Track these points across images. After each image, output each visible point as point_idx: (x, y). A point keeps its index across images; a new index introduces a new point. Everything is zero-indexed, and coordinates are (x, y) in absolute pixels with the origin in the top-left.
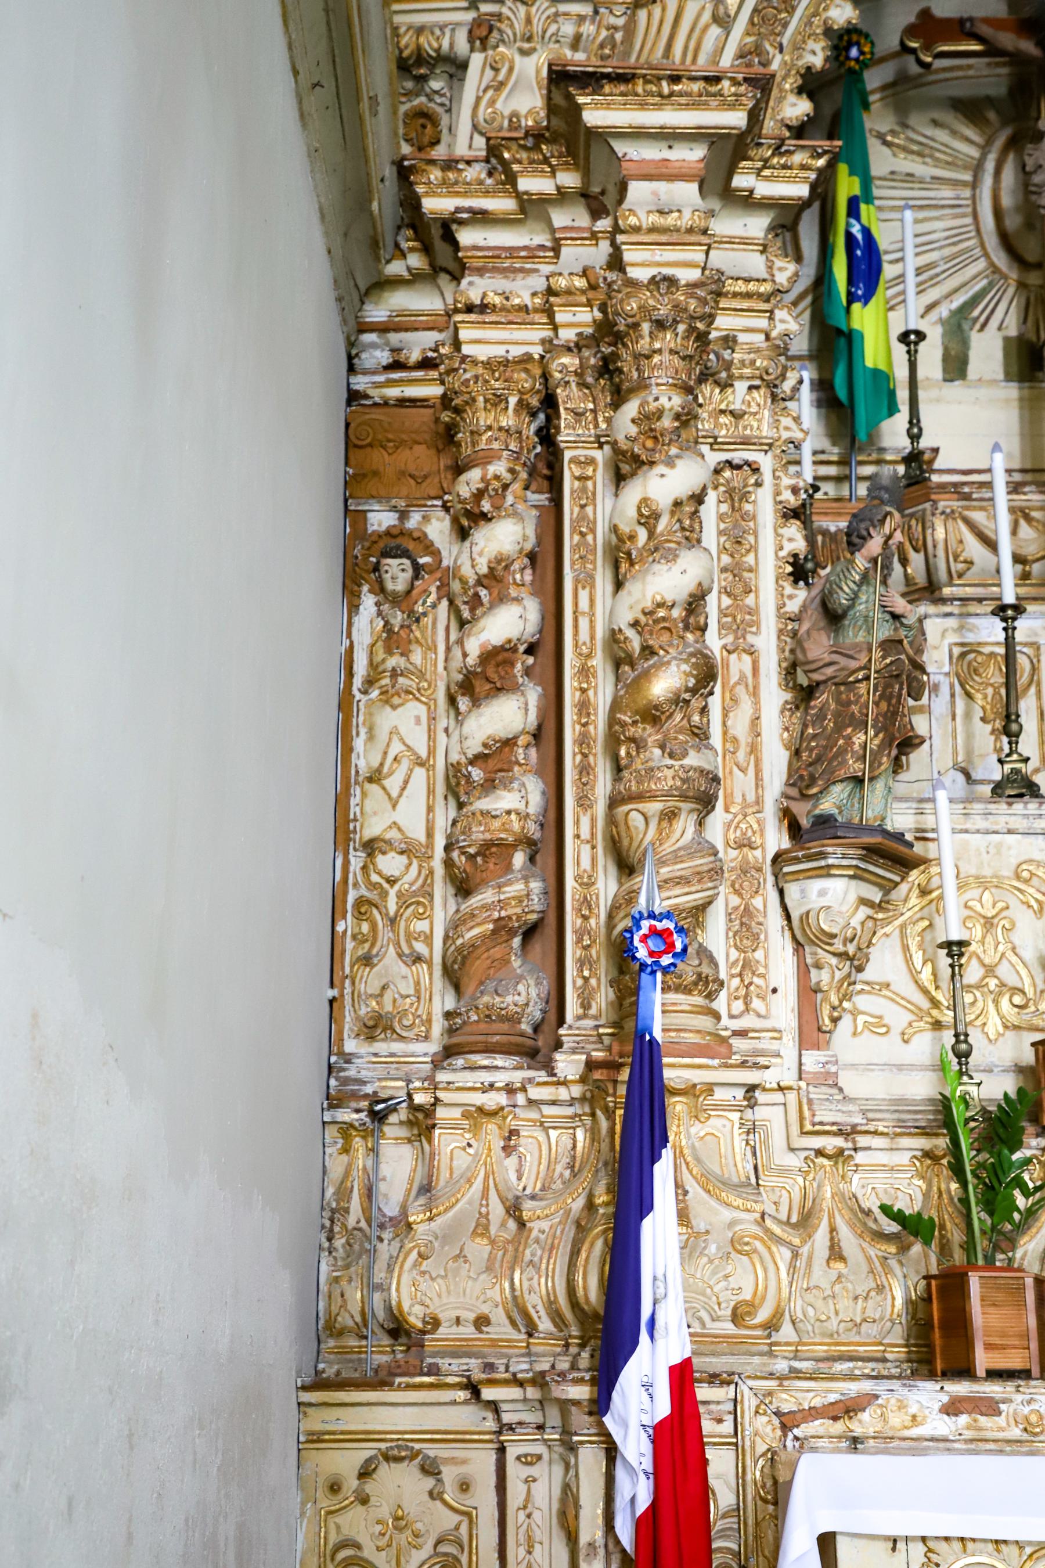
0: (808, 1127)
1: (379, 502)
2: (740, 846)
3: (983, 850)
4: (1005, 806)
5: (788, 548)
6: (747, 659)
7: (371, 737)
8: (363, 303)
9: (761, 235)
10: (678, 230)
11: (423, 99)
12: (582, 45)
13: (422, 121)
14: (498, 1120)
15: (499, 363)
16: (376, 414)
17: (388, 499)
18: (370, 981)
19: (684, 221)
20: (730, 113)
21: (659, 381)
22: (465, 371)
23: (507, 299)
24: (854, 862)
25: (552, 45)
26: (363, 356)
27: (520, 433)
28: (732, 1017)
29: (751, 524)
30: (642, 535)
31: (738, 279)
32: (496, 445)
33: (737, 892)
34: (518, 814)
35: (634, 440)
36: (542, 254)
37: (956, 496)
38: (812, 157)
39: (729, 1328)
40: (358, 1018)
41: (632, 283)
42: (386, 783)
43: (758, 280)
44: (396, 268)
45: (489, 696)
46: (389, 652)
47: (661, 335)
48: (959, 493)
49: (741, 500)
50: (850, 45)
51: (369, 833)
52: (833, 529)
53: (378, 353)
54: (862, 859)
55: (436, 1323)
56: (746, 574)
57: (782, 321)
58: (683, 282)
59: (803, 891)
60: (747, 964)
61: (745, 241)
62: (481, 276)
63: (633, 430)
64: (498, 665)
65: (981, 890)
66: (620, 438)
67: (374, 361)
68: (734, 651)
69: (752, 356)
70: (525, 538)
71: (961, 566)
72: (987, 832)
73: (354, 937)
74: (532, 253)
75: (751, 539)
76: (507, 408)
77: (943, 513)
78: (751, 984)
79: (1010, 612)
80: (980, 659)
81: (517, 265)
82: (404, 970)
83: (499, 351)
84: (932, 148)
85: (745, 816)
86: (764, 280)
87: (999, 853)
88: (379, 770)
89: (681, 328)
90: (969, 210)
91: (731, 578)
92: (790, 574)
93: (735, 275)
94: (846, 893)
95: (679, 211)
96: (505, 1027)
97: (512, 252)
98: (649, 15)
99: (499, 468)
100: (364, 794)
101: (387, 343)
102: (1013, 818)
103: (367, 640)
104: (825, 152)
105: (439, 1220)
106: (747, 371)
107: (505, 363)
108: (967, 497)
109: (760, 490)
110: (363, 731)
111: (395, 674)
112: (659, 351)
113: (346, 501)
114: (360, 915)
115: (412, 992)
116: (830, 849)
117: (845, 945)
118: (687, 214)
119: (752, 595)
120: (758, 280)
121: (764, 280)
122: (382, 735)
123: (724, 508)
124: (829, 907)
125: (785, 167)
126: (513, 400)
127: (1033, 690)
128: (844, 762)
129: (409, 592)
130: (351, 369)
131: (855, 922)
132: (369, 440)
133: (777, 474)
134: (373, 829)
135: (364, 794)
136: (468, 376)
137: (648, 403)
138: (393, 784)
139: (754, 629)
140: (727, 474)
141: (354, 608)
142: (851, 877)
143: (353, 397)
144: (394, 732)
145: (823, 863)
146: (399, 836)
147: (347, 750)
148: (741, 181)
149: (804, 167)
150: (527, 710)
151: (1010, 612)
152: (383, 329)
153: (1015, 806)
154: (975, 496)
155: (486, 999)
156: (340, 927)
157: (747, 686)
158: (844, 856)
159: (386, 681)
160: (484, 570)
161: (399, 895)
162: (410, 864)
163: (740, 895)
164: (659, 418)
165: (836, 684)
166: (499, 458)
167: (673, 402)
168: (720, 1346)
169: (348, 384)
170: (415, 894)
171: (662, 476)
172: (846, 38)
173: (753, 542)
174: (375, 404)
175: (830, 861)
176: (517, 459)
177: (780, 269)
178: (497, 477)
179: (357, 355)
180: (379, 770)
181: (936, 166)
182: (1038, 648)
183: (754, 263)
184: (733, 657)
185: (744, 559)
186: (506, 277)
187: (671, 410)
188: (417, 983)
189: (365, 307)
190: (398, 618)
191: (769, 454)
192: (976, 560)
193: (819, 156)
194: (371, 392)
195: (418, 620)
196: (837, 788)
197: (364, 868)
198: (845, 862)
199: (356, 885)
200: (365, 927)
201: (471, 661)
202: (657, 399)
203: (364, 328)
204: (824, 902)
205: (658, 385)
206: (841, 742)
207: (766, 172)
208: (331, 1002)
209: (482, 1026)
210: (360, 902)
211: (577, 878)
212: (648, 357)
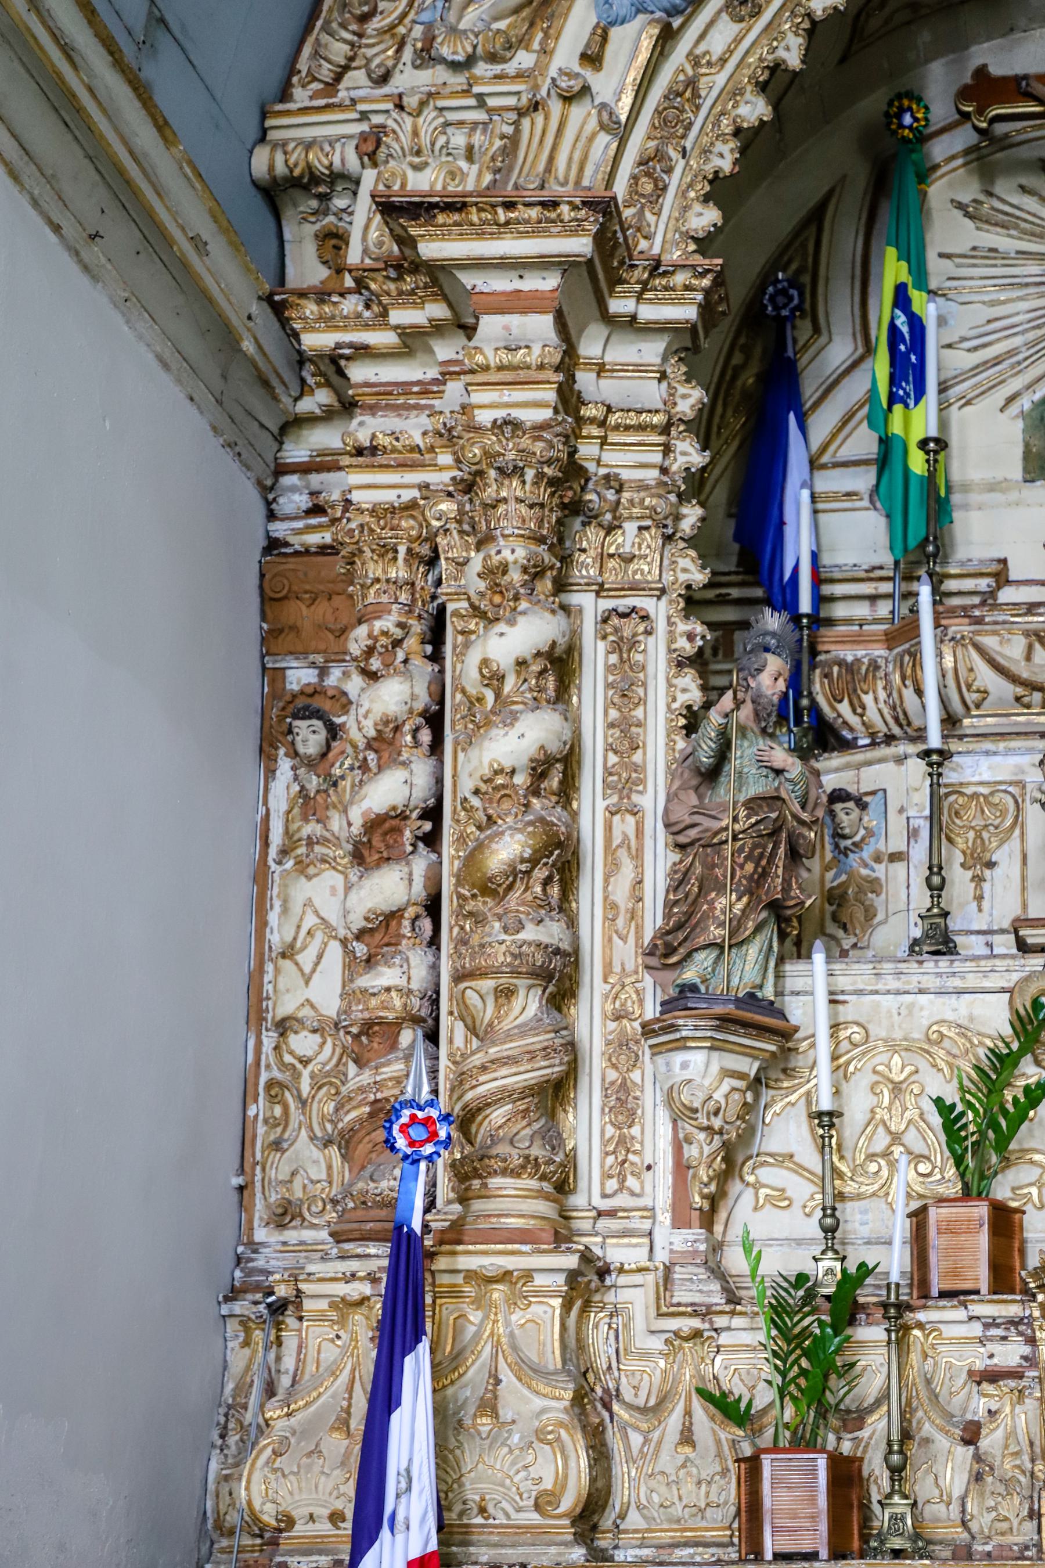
0: (664, 1309)
1: (297, 659)
2: (618, 1018)
3: (895, 1012)
4: (916, 965)
5: (682, 699)
6: (631, 820)
7: (285, 910)
8: (281, 443)
9: (658, 361)
10: (529, 367)
11: (331, 218)
12: (476, 157)
13: (334, 242)
14: (364, 1310)
15: (386, 510)
16: (292, 563)
17: (306, 653)
18: (280, 1167)
19: (534, 357)
20: (574, 239)
21: (506, 532)
22: (349, 520)
23: (397, 439)
24: (709, 1034)
25: (444, 159)
26: (281, 500)
27: (413, 584)
28: (604, 1196)
29: (641, 675)
30: (490, 696)
31: (629, 411)
32: (385, 599)
33: (614, 1066)
34: (399, 991)
35: (482, 595)
36: (435, 389)
38: (695, 277)
39: (535, 1518)
40: (268, 1206)
41: (477, 429)
42: (299, 958)
43: (650, 411)
44: (307, 405)
45: (378, 865)
46: (306, 819)
47: (506, 482)
49: (629, 651)
51: (282, 1012)
52: (850, 658)
53: (296, 497)
54: (717, 1029)
55: (290, 1522)
56: (634, 729)
57: (684, 454)
58: (528, 424)
59: (668, 1064)
60: (622, 1141)
61: (638, 368)
62: (373, 415)
63: (482, 585)
64: (386, 834)
65: (890, 1054)
66: (472, 593)
67: (293, 505)
68: (616, 813)
69: (642, 494)
70: (413, 697)
71: (975, 696)
72: (898, 993)
73: (266, 1121)
74: (426, 389)
75: (641, 691)
76: (395, 559)
77: (953, 639)
78: (624, 1161)
79: (935, 758)
80: (961, 801)
81: (411, 402)
82: (316, 1153)
83: (388, 496)
85: (623, 986)
86: (657, 411)
87: (910, 1014)
88: (292, 946)
89: (530, 474)
91: (618, 733)
92: (684, 727)
93: (625, 406)
94: (707, 1065)
95: (527, 347)
96: (383, 1213)
97: (405, 388)
98: (533, 123)
99: (387, 623)
100: (277, 971)
101: (307, 487)
102: (926, 977)
103: (284, 807)
104: (708, 271)
105: (299, 1416)
106: (636, 511)
107: (392, 510)
109: (651, 639)
110: (277, 904)
111: (310, 842)
112: (505, 500)
113: (263, 657)
114: (272, 1099)
115: (323, 1176)
116: (681, 1022)
117: (708, 1119)
118: (536, 350)
119: (640, 751)
120: (650, 411)
121: (657, 411)
122: (296, 908)
123: (614, 659)
124: (690, 1081)
125: (666, 288)
126: (402, 550)
127: (1017, 832)
128: (707, 928)
129: (324, 755)
130: (271, 516)
131: (719, 1096)
132: (285, 592)
133: (673, 620)
134: (286, 1006)
135: (277, 971)
136: (353, 525)
137: (490, 556)
138: (306, 958)
139: (641, 788)
140: (615, 621)
141: (271, 773)
142: (711, 1048)
143: (273, 545)
144: (308, 903)
145: (678, 1035)
146: (312, 1013)
147: (262, 924)
148: (620, 305)
149: (687, 288)
150: (411, 881)
151: (935, 758)
152: (305, 469)
153: (925, 965)
155: (360, 1185)
156: (251, 1112)
157: (629, 848)
158: (696, 1028)
159: (302, 850)
160: (372, 733)
161: (312, 1076)
162: (324, 1043)
163: (617, 1068)
164: (505, 572)
165: (703, 846)
166: (389, 612)
167: (516, 554)
168: (523, 1537)
169: (267, 532)
170: (328, 1074)
171: (502, 634)
173: (642, 695)
174: (297, 553)
175: (684, 1033)
176: (410, 611)
177: (684, 397)
178: (385, 633)
179: (274, 500)
180: (292, 946)
182: (1024, 787)
183: (652, 393)
184: (617, 818)
185: (633, 713)
186: (399, 415)
187: (515, 562)
188: (330, 1167)
189: (285, 447)
190: (314, 783)
191: (664, 599)
192: (990, 689)
193: (702, 275)
194: (291, 539)
195: (335, 784)
196: (700, 956)
197: (277, 1048)
198: (699, 1034)
199: (268, 1066)
200: (278, 1111)
201: (356, 829)
202: (499, 552)
203: (281, 470)
204: (687, 1075)
205: (503, 536)
206: (705, 907)
207: (648, 295)
208: (241, 1189)
209: (360, 1214)
210: (271, 1084)
211: (451, 1055)
212: (494, 507)
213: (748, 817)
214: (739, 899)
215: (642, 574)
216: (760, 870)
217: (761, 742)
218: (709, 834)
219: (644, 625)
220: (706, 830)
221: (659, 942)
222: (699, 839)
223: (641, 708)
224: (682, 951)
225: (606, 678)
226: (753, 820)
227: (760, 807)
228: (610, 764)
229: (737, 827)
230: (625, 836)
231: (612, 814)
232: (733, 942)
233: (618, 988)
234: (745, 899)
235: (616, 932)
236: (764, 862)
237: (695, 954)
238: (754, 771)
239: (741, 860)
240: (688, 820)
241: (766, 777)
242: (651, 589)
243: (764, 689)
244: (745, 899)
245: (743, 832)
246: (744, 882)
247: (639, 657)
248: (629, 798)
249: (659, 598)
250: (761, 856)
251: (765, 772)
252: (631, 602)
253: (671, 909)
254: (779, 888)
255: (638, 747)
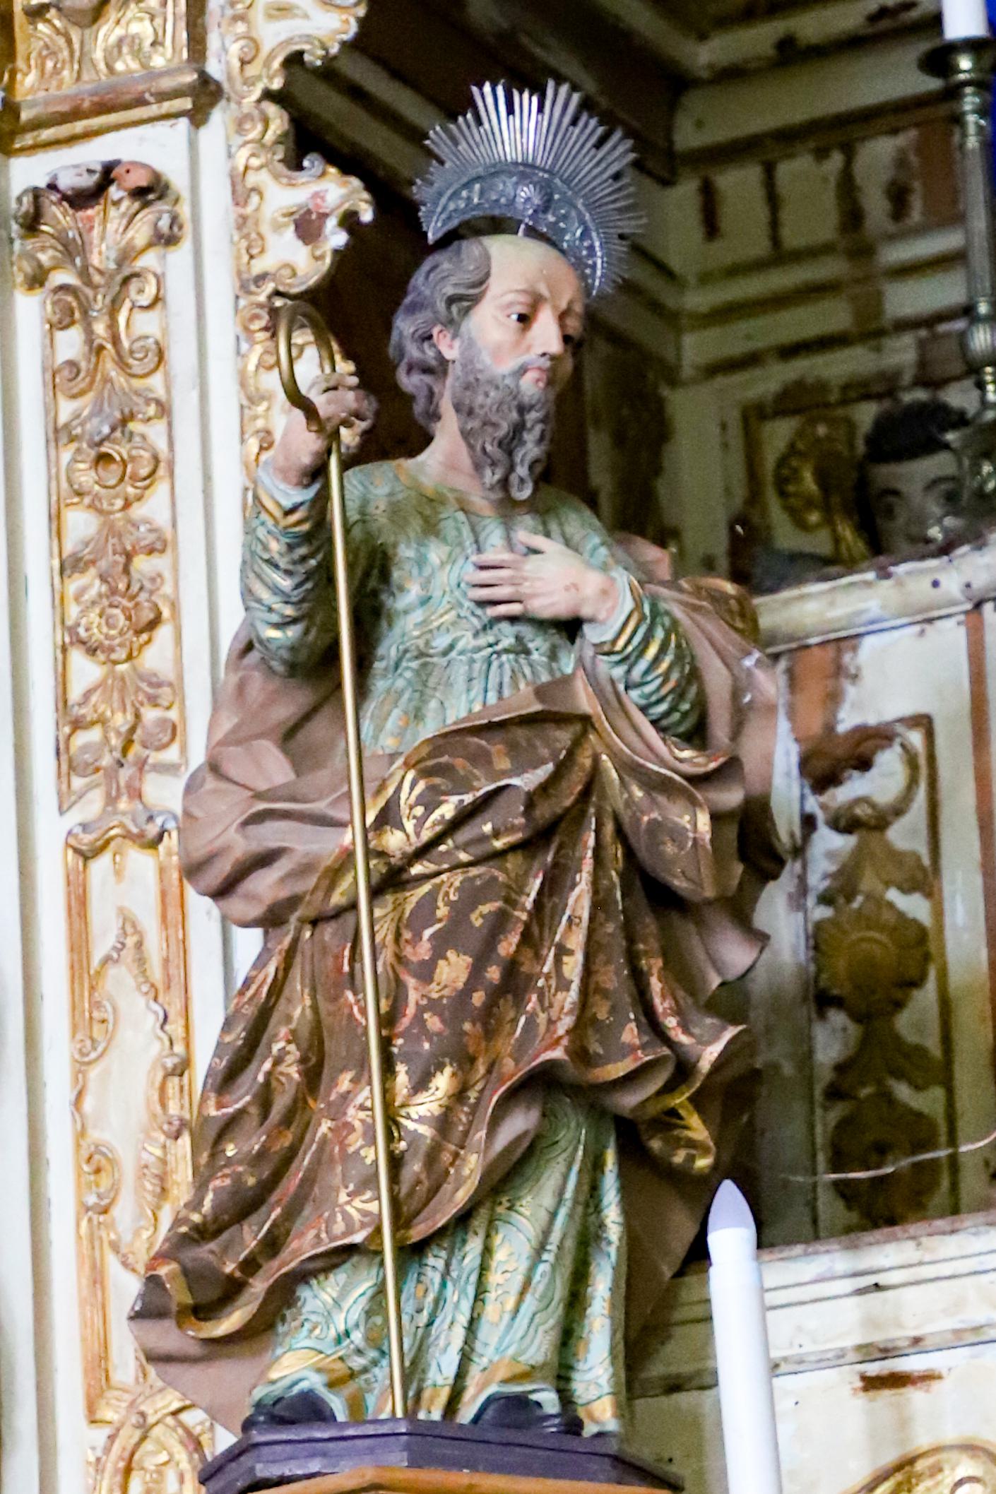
29: (156, 383)
68: (97, 851)
75: (156, 433)
85: (145, 1431)
91: (97, 587)
119: (164, 633)
123: (70, 344)
133: (252, 179)
157: (141, 961)
184: (101, 867)
185: (137, 511)
191: (219, 117)
213: (430, 802)
214: (421, 1084)
215: (137, 53)
216: (494, 974)
217: (494, 535)
218: (312, 881)
219: (147, 216)
220: (304, 870)
221: (163, 1271)
222: (293, 902)
223: (161, 490)
224: (259, 1286)
225: (50, 410)
226: (447, 810)
227: (481, 759)
228: (75, 694)
229: (394, 841)
230: (128, 923)
231: (86, 856)
232: (417, 1232)
233: (129, 1436)
234: (443, 1082)
235: (115, 1247)
236: (508, 945)
237: (304, 1293)
238: (467, 641)
239: (423, 950)
240: (242, 846)
241: (521, 649)
242: (163, 96)
243: (486, 359)
244: (443, 1082)
245: (423, 852)
246: (434, 1022)
247: (147, 324)
248: (136, 794)
249: (198, 117)
250: (499, 923)
251: (507, 635)
252: (96, 152)
253: (215, 1154)
254: (566, 1022)
255: (153, 624)
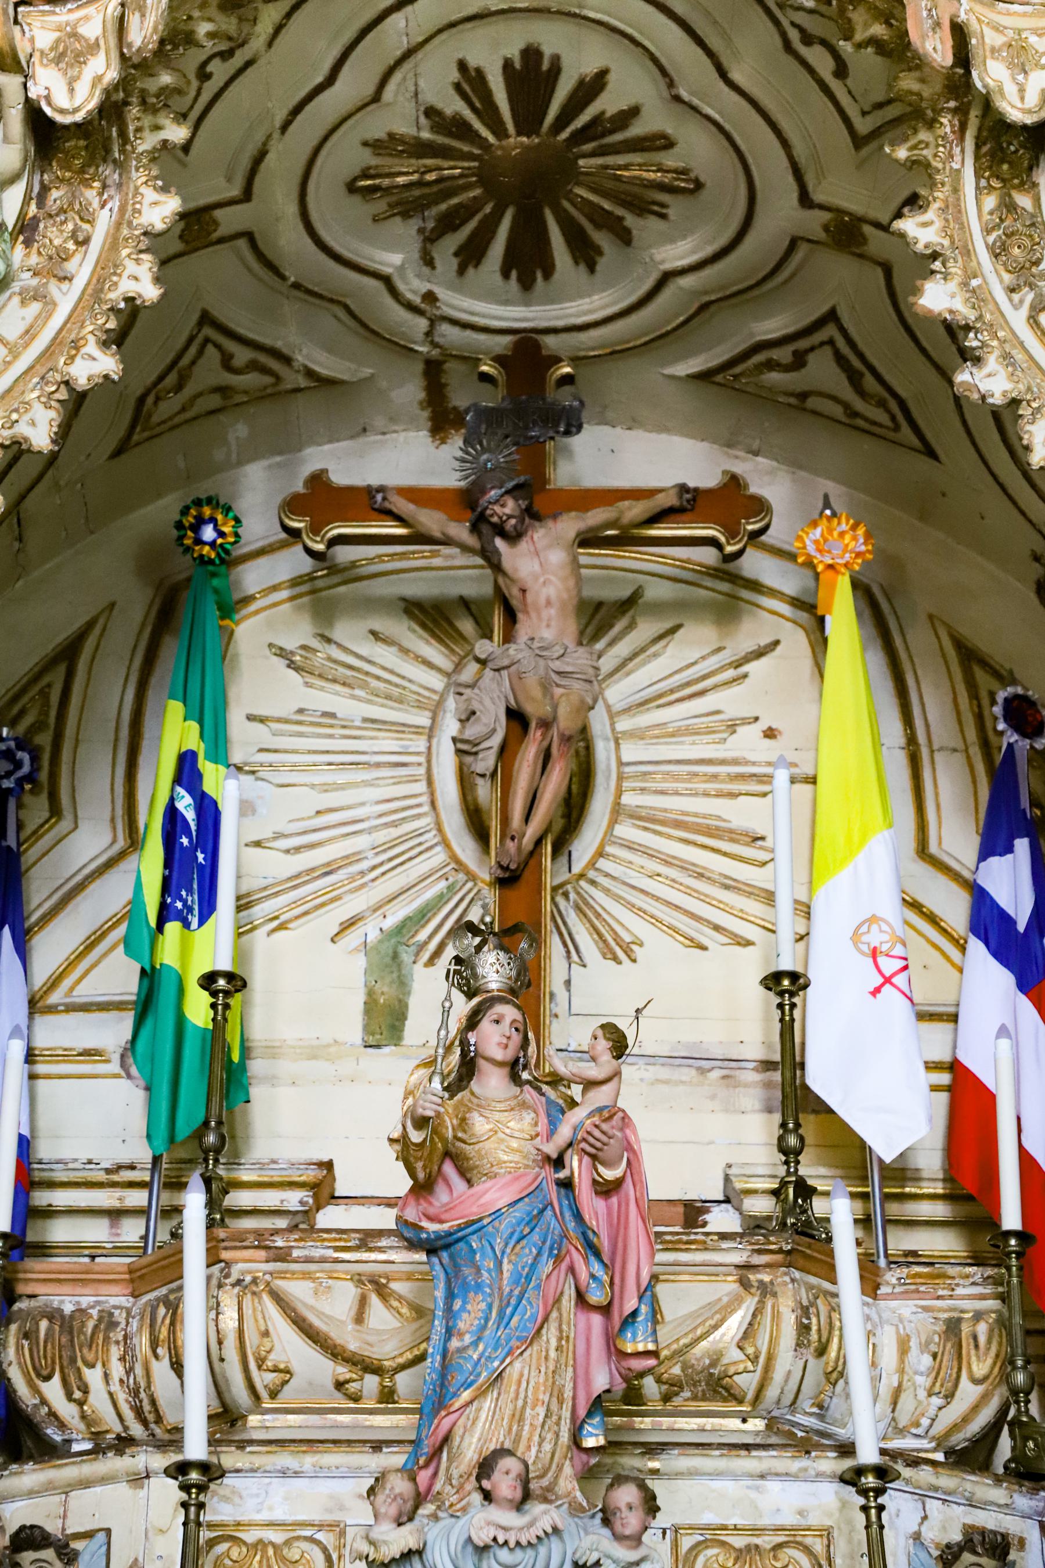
37: (262, 1254)
48: (267, 1248)
50: (200, 522)
84: (367, 673)
90: (422, 770)
108: (282, 1256)
154: (295, 1253)
172: (193, 512)
181: (369, 702)
